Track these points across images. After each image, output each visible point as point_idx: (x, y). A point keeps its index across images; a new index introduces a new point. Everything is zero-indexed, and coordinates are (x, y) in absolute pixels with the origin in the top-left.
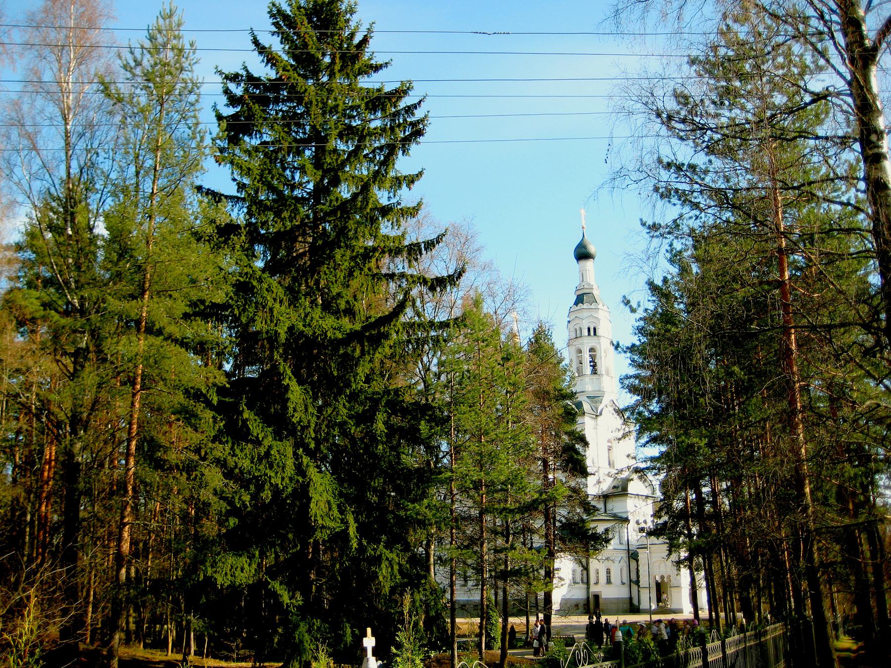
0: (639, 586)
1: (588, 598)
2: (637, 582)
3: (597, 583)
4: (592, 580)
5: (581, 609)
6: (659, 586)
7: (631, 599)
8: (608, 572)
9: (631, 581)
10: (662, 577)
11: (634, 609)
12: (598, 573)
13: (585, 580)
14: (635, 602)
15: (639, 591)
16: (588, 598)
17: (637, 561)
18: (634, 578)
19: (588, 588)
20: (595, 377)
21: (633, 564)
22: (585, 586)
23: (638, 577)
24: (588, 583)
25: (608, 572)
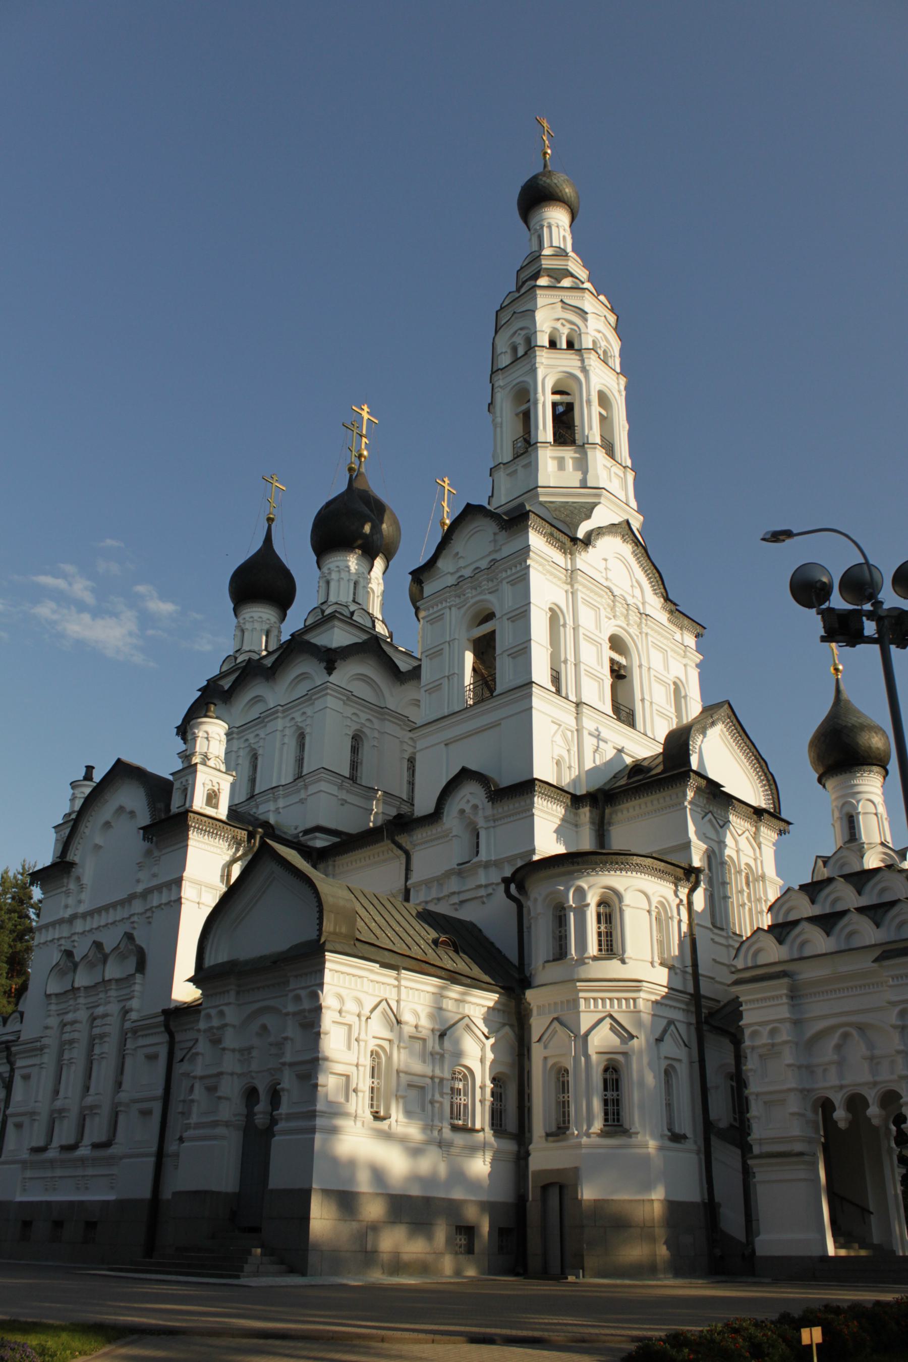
0: (745, 1149)
2: (738, 1133)
4: (539, 1125)
7: (710, 1207)
9: (708, 1127)
12: (563, 1087)
13: (511, 1123)
14: (732, 1221)
15: (747, 1173)
16: (521, 1200)
17: (736, 1039)
18: (721, 1112)
19: (521, 1158)
20: (568, 454)
21: (719, 1055)
22: (510, 1146)
23: (740, 1103)
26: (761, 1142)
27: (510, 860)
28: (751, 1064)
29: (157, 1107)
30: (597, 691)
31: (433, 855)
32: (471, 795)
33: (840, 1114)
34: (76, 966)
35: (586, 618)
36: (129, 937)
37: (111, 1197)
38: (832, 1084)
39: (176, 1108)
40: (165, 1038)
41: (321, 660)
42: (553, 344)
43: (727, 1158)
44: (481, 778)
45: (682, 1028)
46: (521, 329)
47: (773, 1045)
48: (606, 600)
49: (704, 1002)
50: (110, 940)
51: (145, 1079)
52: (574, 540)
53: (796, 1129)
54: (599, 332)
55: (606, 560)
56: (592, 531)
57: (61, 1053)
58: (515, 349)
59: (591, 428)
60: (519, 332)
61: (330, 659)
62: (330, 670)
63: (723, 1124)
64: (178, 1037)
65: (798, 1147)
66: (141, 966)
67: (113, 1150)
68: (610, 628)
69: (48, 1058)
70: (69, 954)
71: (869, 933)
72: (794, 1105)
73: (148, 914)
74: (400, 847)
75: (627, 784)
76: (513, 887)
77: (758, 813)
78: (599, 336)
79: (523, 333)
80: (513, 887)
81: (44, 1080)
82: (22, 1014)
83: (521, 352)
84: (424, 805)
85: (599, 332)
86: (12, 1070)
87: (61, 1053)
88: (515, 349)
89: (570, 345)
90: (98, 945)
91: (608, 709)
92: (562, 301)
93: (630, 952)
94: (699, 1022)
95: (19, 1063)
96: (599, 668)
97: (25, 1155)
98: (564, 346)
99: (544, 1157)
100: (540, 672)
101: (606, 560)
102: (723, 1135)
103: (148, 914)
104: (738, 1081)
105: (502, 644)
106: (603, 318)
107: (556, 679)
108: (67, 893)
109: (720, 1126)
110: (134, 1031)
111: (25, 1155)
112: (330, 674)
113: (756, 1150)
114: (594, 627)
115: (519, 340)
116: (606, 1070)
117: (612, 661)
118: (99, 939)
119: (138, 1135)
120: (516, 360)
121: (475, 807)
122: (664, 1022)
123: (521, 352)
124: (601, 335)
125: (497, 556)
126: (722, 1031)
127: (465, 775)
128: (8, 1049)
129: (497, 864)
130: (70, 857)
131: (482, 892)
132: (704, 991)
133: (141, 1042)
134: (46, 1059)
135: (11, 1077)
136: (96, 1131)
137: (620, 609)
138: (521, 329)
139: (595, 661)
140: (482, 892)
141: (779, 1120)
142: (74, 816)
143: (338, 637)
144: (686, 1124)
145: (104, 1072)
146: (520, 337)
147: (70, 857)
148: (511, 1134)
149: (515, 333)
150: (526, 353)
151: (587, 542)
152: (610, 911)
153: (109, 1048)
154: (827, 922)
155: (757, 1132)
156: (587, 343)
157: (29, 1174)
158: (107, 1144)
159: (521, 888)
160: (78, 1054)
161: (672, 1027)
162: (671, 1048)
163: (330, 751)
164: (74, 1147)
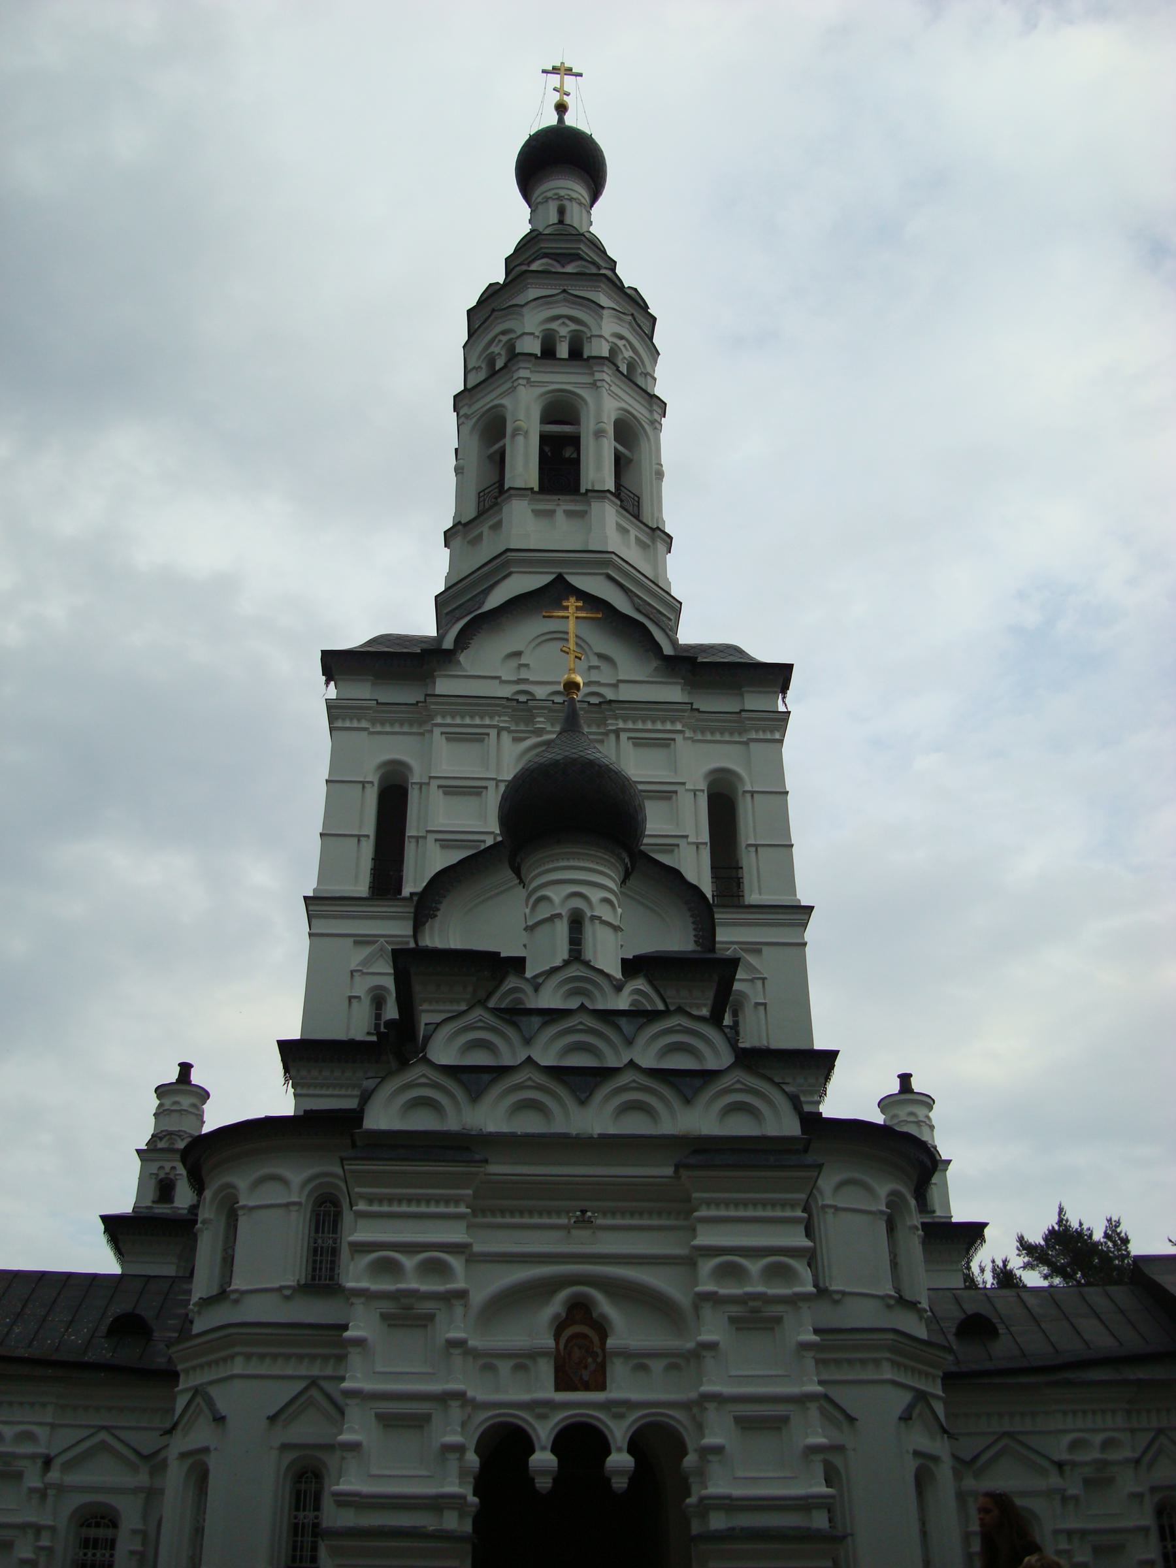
20: (562, 505)
42: (548, 352)
46: (504, 333)
54: (621, 337)
59: (599, 468)
79: (504, 338)
83: (499, 364)
85: (621, 337)
88: (491, 361)
89: (576, 353)
92: (564, 291)
120: (493, 374)
123: (499, 364)
124: (623, 342)
138: (504, 333)
146: (501, 344)
149: (496, 336)
150: (505, 366)
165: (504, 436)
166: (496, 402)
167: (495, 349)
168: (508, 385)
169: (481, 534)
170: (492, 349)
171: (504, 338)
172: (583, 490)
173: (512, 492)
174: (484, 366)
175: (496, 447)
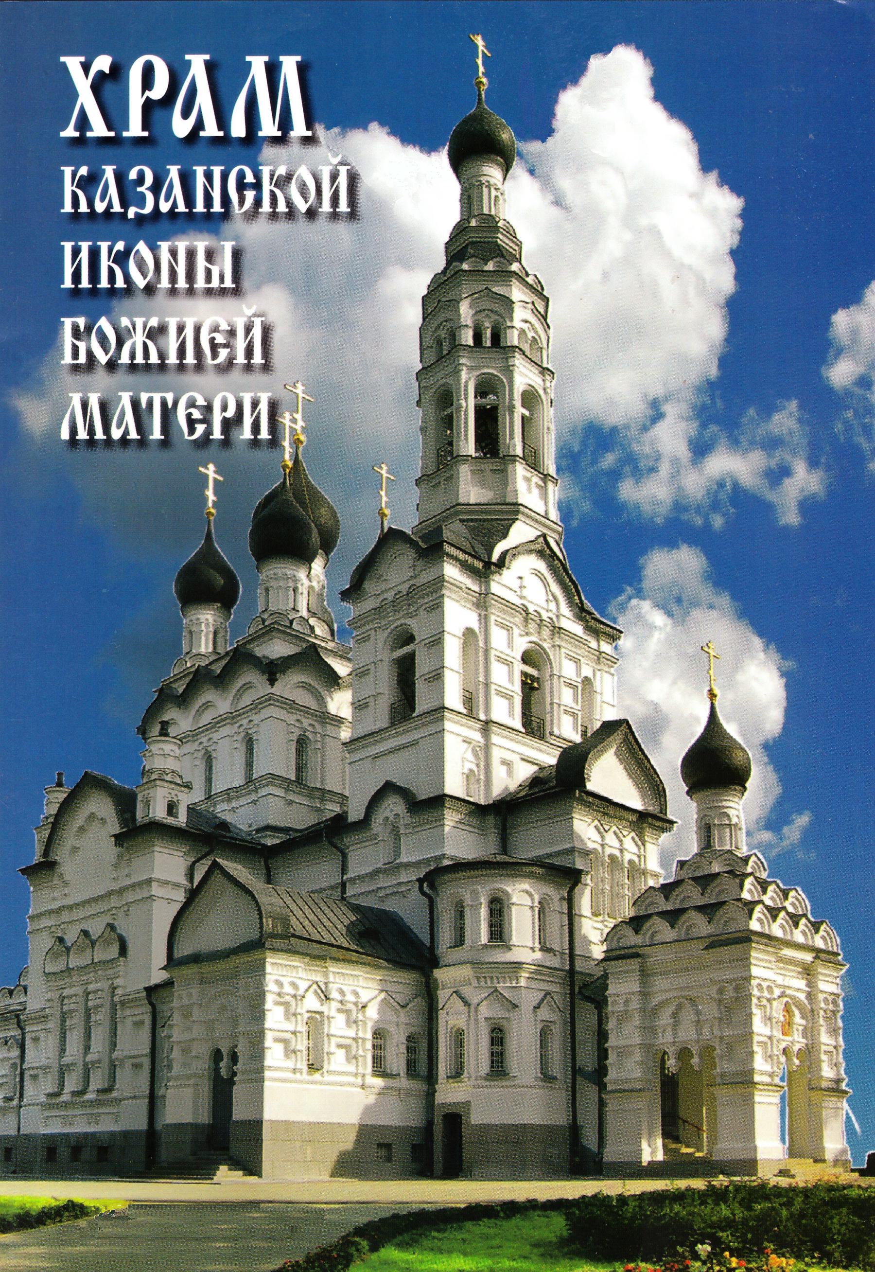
0: (602, 1086)
1: (430, 1124)
3: (457, 1074)
5: (402, 1153)
6: (670, 1087)
7: (575, 1129)
8: (498, 1036)
9: (576, 1071)
10: (684, 1054)
11: (583, 1162)
13: (423, 1069)
14: (590, 1140)
15: (602, 1103)
16: (430, 1124)
18: (587, 1059)
19: (430, 1094)
20: (489, 465)
21: (587, 1016)
23: (603, 1054)
24: (431, 1078)
25: (498, 1036)
26: (616, 1082)
27: (427, 861)
28: (611, 1025)
29: (146, 1062)
30: (506, 710)
31: (364, 857)
32: (394, 806)
33: (672, 1063)
34: (68, 949)
35: (498, 638)
36: (112, 927)
37: (116, 1128)
38: (665, 1040)
39: (161, 1063)
40: (149, 1008)
41: (263, 673)
43: (588, 1092)
44: (404, 793)
45: (557, 998)
46: (446, 321)
47: (626, 1011)
48: (519, 619)
49: (577, 976)
50: (96, 928)
51: (134, 1042)
52: (488, 564)
53: (638, 1073)
54: (526, 321)
55: (520, 578)
56: (507, 551)
57: (63, 1021)
58: (440, 343)
59: (512, 437)
60: (445, 323)
61: (273, 670)
62: (272, 681)
63: (590, 1069)
64: (159, 1007)
65: (639, 1086)
66: (123, 951)
67: (114, 1094)
68: (522, 644)
69: (53, 1024)
70: (61, 940)
71: (702, 926)
72: (638, 1056)
73: (125, 908)
74: (336, 847)
75: (526, 795)
76: (425, 884)
77: (643, 816)
78: (525, 326)
79: (448, 325)
80: (425, 884)
81: (50, 1043)
82: (25, 988)
84: (355, 813)
85: (526, 321)
86: (23, 1034)
87: (63, 1021)
88: (440, 343)
90: (86, 933)
91: (517, 724)
93: (515, 940)
94: (572, 994)
95: (28, 1029)
96: (509, 686)
97: (43, 1099)
98: (488, 343)
99: (448, 1093)
100: (453, 697)
101: (520, 578)
102: (588, 1077)
103: (125, 908)
104: (602, 1036)
105: (422, 667)
106: (530, 306)
107: (469, 700)
108: (53, 888)
109: (585, 1071)
110: (123, 1003)
111: (43, 1099)
112: (272, 685)
113: (609, 1087)
114: (508, 643)
115: (443, 333)
116: (493, 1031)
117: (524, 674)
118: (86, 928)
119: (132, 1083)
120: (440, 358)
121: (397, 815)
122: (542, 994)
124: (528, 325)
125: (419, 581)
126: (589, 999)
127: (388, 788)
128: (18, 1016)
129: (416, 864)
130: (52, 857)
131: (403, 888)
132: (578, 968)
133: (128, 1012)
134: (50, 1025)
135: (23, 1039)
136: (97, 1081)
137: (532, 627)
138: (446, 321)
139: (506, 678)
140: (403, 888)
141: (628, 1068)
142: (51, 820)
143: (277, 649)
144: (557, 1068)
145: (99, 1036)
146: (445, 330)
147: (52, 857)
148: (422, 1077)
151: (501, 564)
152: (498, 909)
153: (101, 1017)
154: (673, 916)
155: (612, 1075)
156: (513, 338)
157: (47, 1114)
158: (109, 1090)
159: (432, 886)
160: (76, 1022)
161: (549, 997)
162: (545, 1013)
163: (275, 758)
164: (83, 1092)
165: (452, 405)
166: (442, 382)
167: (443, 333)
168: (450, 369)
169: (439, 482)
170: (439, 332)
171: (448, 325)
172: (501, 456)
173: (460, 458)
174: (434, 345)
175: (448, 411)
